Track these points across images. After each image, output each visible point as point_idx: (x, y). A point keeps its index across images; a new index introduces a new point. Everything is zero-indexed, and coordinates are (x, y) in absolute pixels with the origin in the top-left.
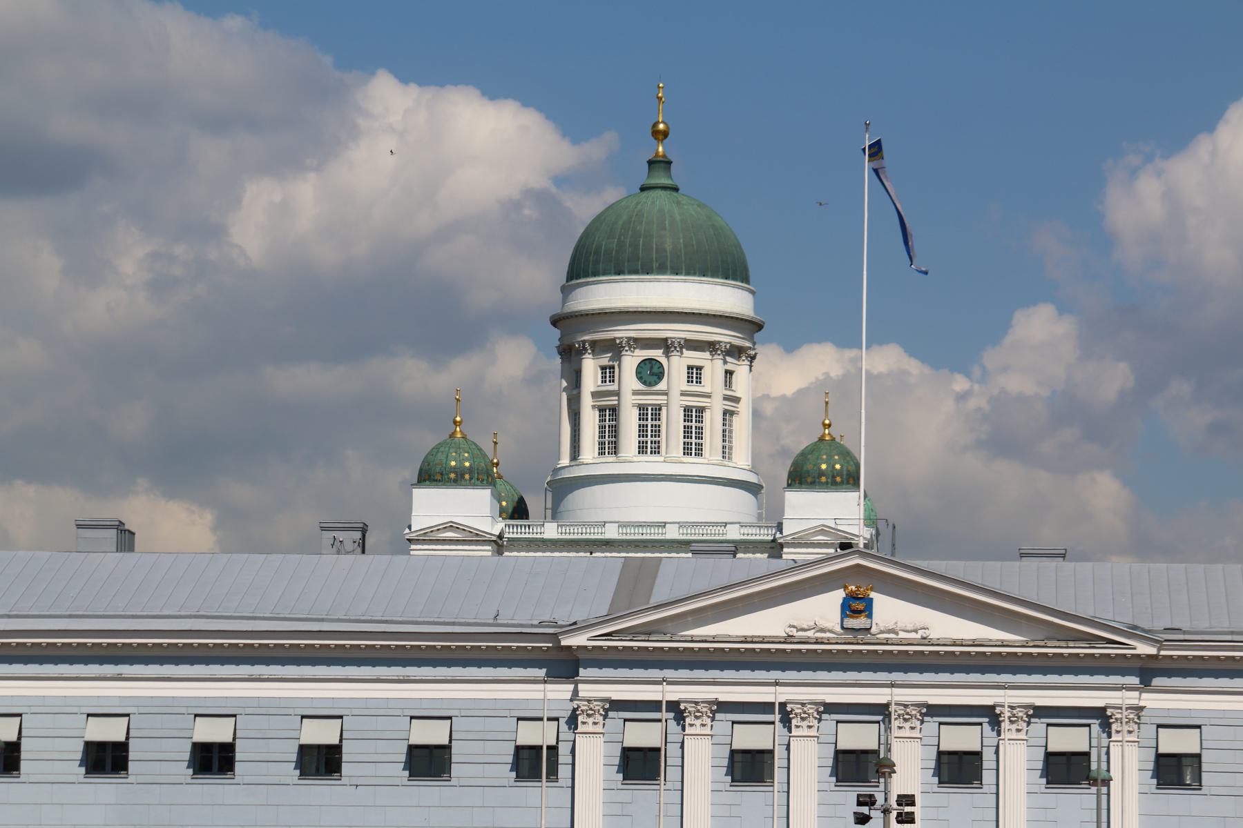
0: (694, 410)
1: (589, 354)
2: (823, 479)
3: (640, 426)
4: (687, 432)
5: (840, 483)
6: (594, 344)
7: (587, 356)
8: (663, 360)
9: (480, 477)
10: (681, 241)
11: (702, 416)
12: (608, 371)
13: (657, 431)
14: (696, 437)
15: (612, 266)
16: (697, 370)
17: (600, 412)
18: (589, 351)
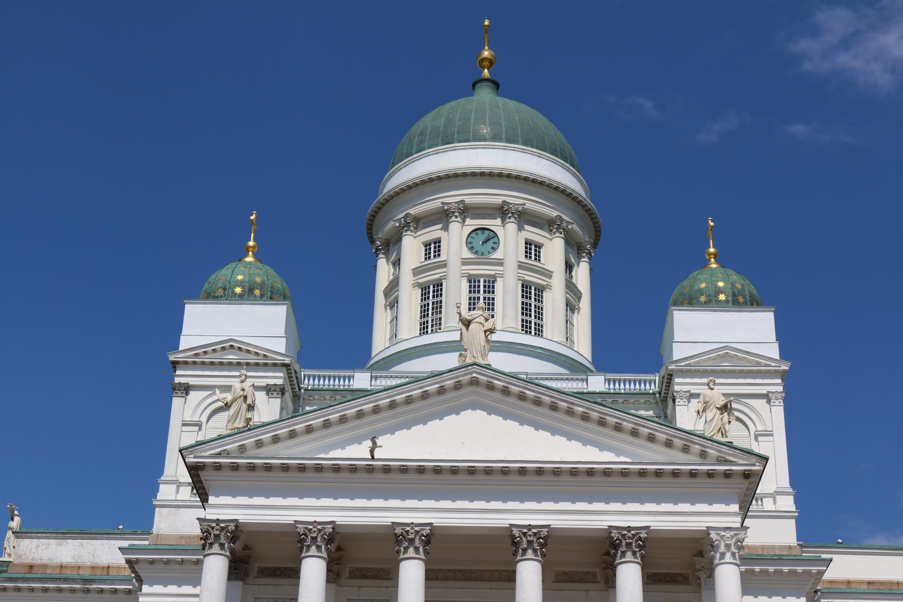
0: (533, 288)
1: (412, 231)
2: (722, 297)
3: (470, 299)
4: (525, 309)
5: (743, 303)
7: (409, 233)
8: (499, 231)
9: (274, 296)
10: (517, 118)
11: (542, 296)
12: (433, 246)
14: (535, 317)
15: (440, 141)
16: (536, 246)
17: (422, 291)
18: (412, 228)
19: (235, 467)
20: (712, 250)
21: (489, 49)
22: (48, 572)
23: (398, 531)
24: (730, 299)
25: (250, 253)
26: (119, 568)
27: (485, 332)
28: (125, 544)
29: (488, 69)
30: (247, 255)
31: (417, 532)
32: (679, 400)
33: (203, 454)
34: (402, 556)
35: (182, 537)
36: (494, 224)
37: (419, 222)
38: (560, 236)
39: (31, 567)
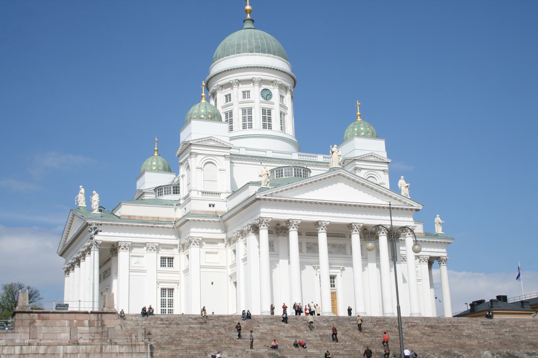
2: (369, 134)
6: (240, 82)
10: (274, 44)
12: (246, 92)
13: (270, 120)
19: (270, 200)
20: (358, 113)
21: (250, 5)
22: (136, 219)
23: (320, 223)
24: (371, 135)
25: (203, 98)
27: (338, 156)
29: (249, 13)
30: (201, 100)
31: (325, 224)
32: (357, 170)
33: (262, 195)
34: (320, 231)
35: (202, 211)
36: (270, 87)
37: (240, 82)
38: (277, 87)
39: (129, 216)
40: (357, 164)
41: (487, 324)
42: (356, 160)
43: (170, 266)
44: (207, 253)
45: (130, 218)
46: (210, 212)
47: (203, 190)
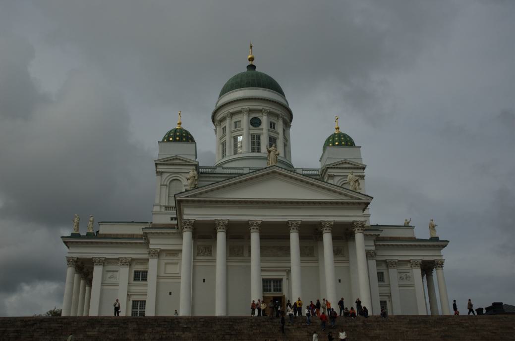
2: (343, 143)
13: (259, 144)
19: (193, 201)
22: (112, 236)
26: (137, 235)
28: (144, 227)
34: (252, 231)
35: (163, 224)
37: (232, 114)
39: (105, 235)
40: (330, 172)
41: (415, 323)
42: (328, 168)
43: (144, 280)
44: (166, 264)
45: (106, 236)
46: (171, 224)
47: (167, 205)
